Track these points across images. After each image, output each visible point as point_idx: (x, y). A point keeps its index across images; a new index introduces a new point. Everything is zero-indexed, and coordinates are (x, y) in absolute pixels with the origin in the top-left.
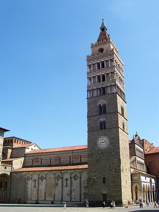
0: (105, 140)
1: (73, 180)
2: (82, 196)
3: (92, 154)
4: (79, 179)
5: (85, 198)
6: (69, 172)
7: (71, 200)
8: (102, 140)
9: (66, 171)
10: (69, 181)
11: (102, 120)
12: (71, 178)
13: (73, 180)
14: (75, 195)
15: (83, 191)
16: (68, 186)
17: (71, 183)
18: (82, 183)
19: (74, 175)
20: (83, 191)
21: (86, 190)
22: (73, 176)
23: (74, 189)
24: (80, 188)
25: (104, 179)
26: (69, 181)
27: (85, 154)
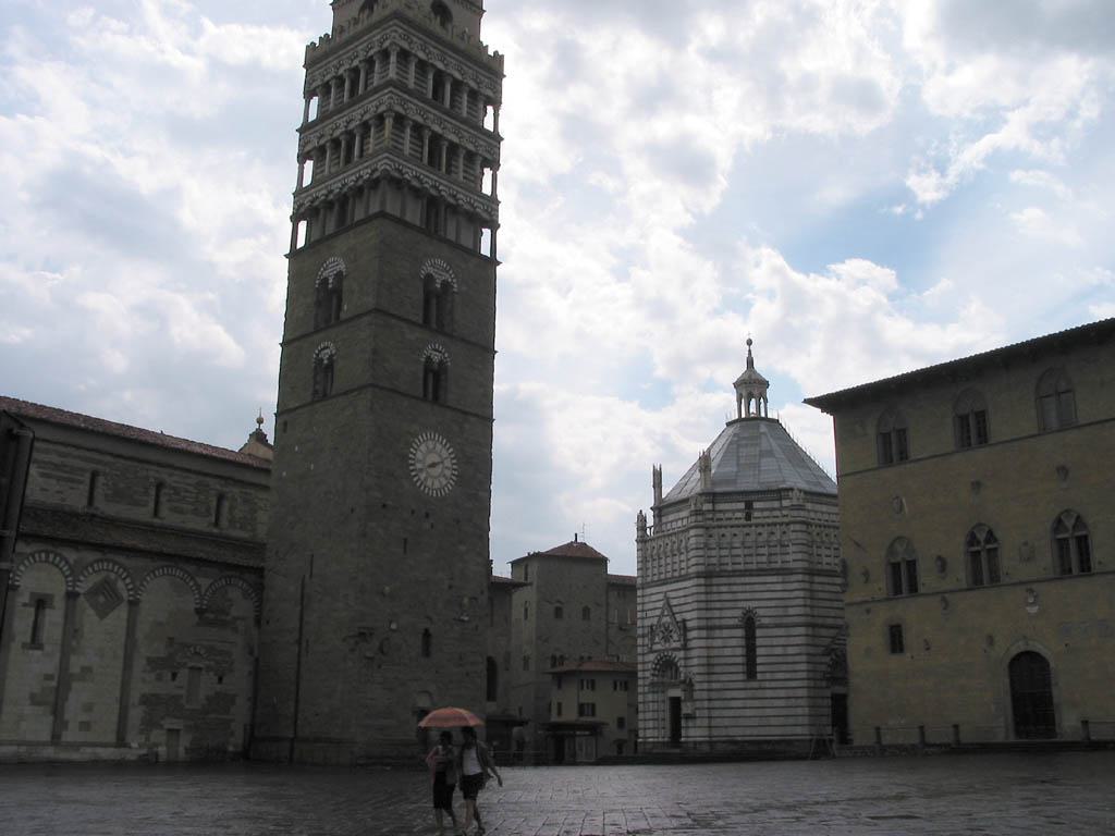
0: (440, 456)
1: (88, 616)
2: (136, 714)
3: (384, 506)
4: (122, 612)
5: (149, 724)
6: (72, 556)
7: (55, 739)
8: (430, 451)
9: (50, 548)
10: (54, 617)
11: (436, 357)
12: (71, 596)
13: (88, 616)
14: (88, 708)
15: (144, 682)
16: (48, 648)
17: (71, 631)
18: (139, 635)
19: (94, 579)
20: (144, 683)
21: (159, 678)
22: (82, 588)
23: (87, 670)
24: (128, 666)
25: (427, 634)
26: (54, 617)
27: (56, 459)
